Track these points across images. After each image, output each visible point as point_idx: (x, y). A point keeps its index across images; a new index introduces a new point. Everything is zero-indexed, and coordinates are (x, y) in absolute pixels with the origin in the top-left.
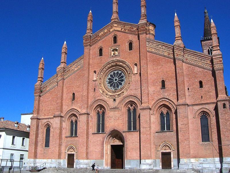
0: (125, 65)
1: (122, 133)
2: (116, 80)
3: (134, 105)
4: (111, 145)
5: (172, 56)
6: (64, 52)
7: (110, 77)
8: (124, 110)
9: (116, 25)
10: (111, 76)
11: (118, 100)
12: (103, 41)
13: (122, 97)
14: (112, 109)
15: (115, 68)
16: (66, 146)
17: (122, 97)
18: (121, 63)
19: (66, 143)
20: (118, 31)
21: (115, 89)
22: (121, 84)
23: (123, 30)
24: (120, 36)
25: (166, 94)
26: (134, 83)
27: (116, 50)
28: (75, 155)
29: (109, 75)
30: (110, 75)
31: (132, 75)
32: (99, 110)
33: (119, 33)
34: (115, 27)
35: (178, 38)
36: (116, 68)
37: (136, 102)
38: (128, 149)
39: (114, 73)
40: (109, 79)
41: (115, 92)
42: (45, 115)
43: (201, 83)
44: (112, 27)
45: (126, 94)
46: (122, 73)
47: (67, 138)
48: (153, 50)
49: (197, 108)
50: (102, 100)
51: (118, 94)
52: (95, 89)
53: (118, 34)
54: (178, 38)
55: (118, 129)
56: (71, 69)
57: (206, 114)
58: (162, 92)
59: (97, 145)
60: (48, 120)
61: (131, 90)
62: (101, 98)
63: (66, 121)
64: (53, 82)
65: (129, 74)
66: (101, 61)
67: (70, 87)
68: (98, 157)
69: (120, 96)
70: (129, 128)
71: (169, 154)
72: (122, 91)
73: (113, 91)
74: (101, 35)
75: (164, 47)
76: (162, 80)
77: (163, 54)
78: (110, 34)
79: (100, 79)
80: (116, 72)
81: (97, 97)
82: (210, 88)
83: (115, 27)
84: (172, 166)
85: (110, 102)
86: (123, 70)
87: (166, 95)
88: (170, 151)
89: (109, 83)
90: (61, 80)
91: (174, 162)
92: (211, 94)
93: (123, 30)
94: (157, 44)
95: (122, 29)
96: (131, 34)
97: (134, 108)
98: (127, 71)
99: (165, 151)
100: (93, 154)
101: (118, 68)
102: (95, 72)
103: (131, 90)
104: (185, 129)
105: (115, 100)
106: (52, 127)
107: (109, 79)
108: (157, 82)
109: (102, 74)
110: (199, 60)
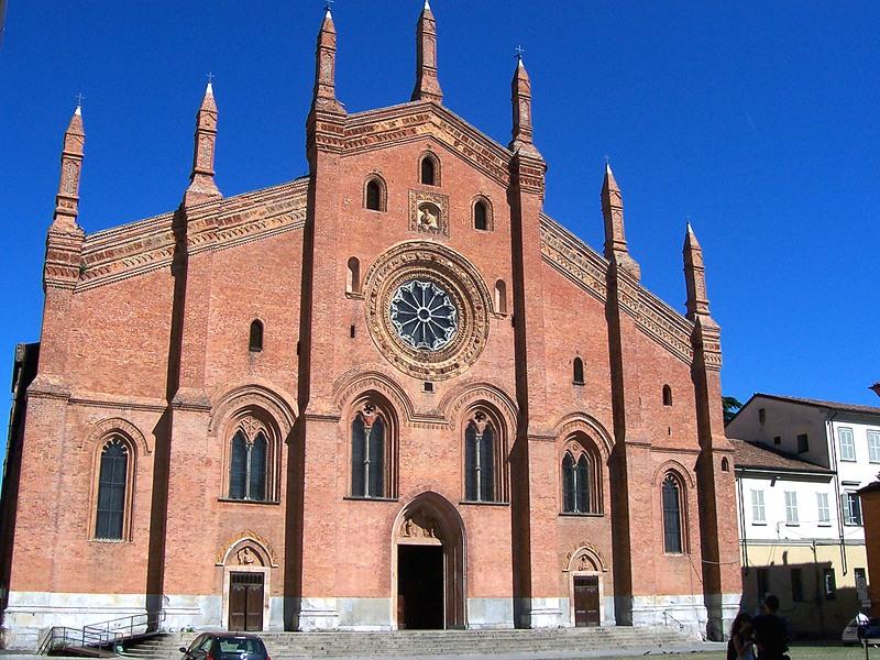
0: (464, 275)
1: (456, 505)
3: (489, 418)
4: (399, 545)
5: (603, 293)
6: (208, 128)
8: (460, 428)
9: (434, 119)
10: (407, 294)
11: (441, 388)
12: (387, 158)
14: (423, 416)
15: (424, 272)
16: (223, 541)
17: (454, 379)
18: (451, 264)
19: (220, 525)
20: (443, 144)
21: (421, 344)
22: (442, 334)
23: (460, 148)
24: (448, 164)
25: (586, 403)
26: (495, 344)
27: (434, 210)
28: (267, 579)
31: (490, 315)
32: (365, 413)
34: (435, 125)
35: (620, 246)
36: (428, 273)
37: (501, 409)
38: (475, 564)
39: (418, 289)
40: (399, 304)
41: (425, 358)
42: (97, 386)
43: (667, 390)
44: (422, 121)
45: (466, 372)
47: (225, 506)
48: (554, 256)
49: (659, 458)
50: (385, 377)
51: (438, 366)
52: (353, 328)
53: (443, 154)
54: (620, 246)
55: (442, 491)
56: (247, 216)
57: (124, 441)
58: (575, 395)
59: (366, 542)
60: (117, 413)
61: (486, 364)
62: (381, 368)
63: (220, 431)
64: (149, 243)
65: (479, 308)
66: (379, 228)
67: (239, 289)
68: (369, 588)
69: (448, 377)
70: (471, 494)
71: (594, 581)
72: (451, 361)
73: (415, 353)
74: (380, 129)
75: (584, 259)
76: (575, 356)
77: (580, 277)
78: (412, 140)
79: (373, 295)
82: (687, 410)
83: (435, 125)
84: (602, 618)
85: (414, 388)
86: (453, 289)
87: (586, 406)
88: (595, 573)
89: (400, 318)
90: (205, 250)
91: (607, 606)
92: (689, 426)
93: (460, 148)
94: (565, 240)
95: (457, 144)
96: (487, 173)
97: (487, 431)
98: (469, 297)
99: (582, 573)
100: (349, 576)
101: (433, 274)
102: (354, 264)
103: (486, 364)
104: (643, 515)
105: (429, 387)
106: (141, 449)
107: (399, 304)
109: (380, 277)
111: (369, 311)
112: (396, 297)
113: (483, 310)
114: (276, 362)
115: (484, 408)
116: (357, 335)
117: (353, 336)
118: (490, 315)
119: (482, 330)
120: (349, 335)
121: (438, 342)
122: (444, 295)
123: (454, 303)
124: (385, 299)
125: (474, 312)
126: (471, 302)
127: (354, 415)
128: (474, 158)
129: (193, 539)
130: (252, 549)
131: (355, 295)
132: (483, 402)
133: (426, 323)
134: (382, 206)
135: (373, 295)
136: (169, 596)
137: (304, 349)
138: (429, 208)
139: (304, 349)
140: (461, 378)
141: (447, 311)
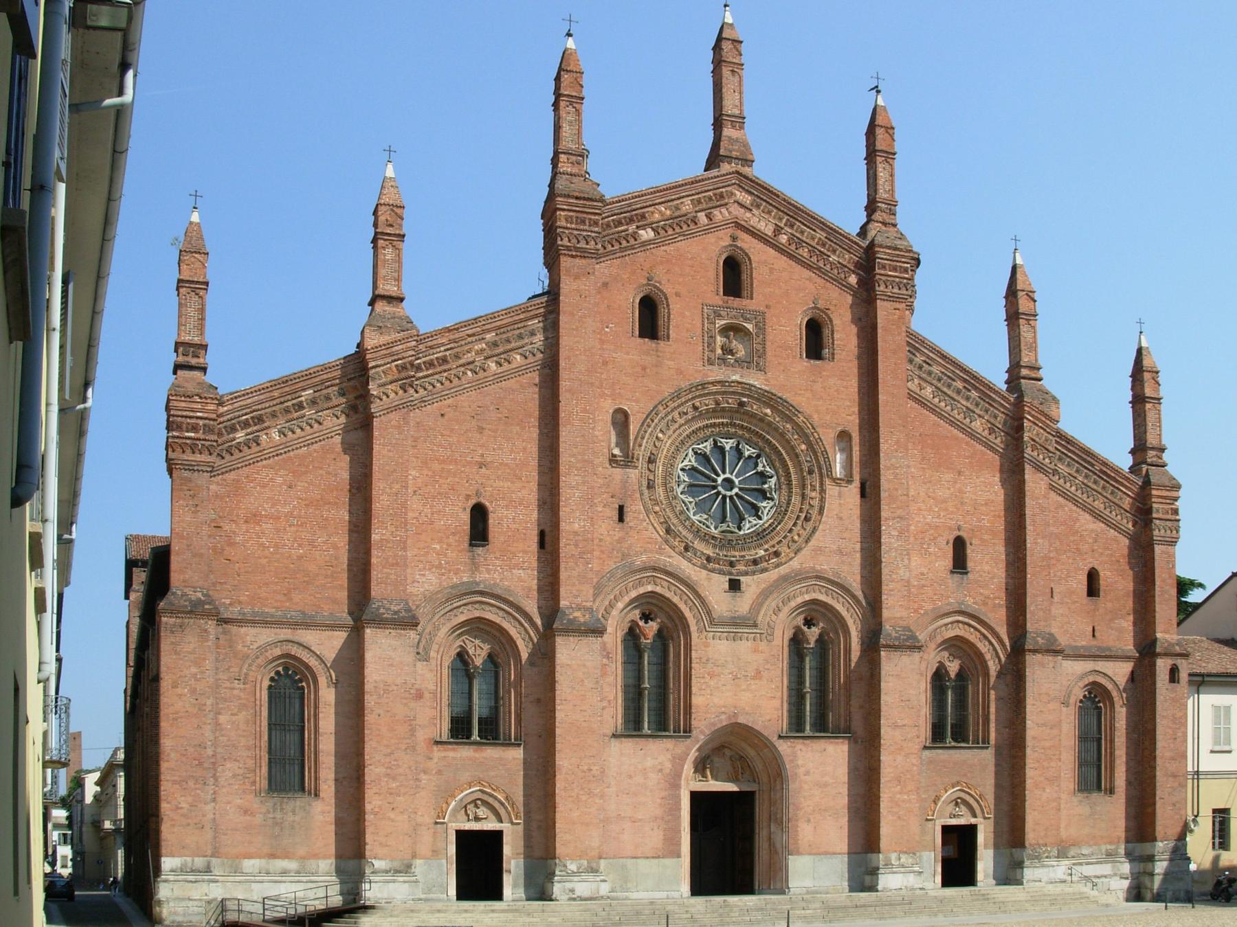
2: (729, 483)
7: (693, 460)
10: (703, 457)
11: (752, 585)
13: (773, 575)
21: (724, 527)
29: (690, 449)
30: (696, 453)
33: (760, 246)
46: (758, 456)
63: (433, 654)
76: (957, 533)
78: (707, 231)
80: (728, 444)
81: (637, 554)
87: (971, 603)
97: (821, 641)
105: (735, 586)
108: (935, 538)
109: (660, 435)
110: (1095, 487)
111: (645, 483)
112: (686, 462)
113: (816, 475)
114: (511, 559)
115: (814, 613)
116: (627, 518)
117: (621, 519)
118: (827, 481)
119: (816, 503)
120: (616, 518)
121: (750, 525)
122: (758, 456)
123: (771, 464)
124: (671, 465)
125: (803, 479)
126: (798, 465)
127: (627, 626)
128: (804, 252)
129: (403, 790)
130: (485, 803)
131: (627, 460)
132: (814, 602)
133: (731, 497)
134: (661, 333)
135: (651, 461)
136: (373, 861)
137: (548, 541)
138: (732, 330)
139: (548, 541)
140: (783, 570)
141: (763, 476)
